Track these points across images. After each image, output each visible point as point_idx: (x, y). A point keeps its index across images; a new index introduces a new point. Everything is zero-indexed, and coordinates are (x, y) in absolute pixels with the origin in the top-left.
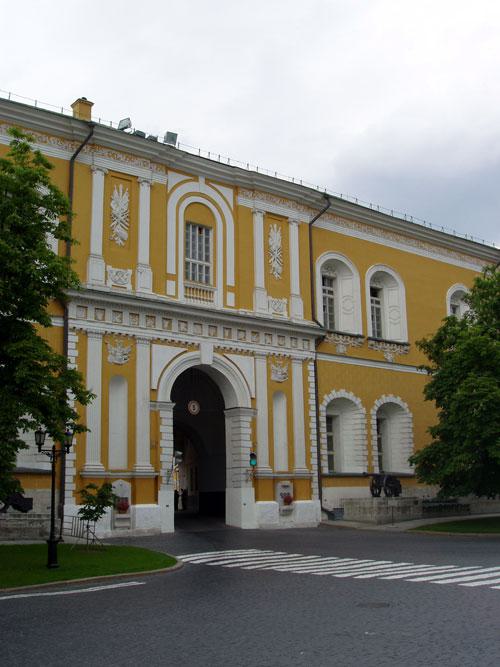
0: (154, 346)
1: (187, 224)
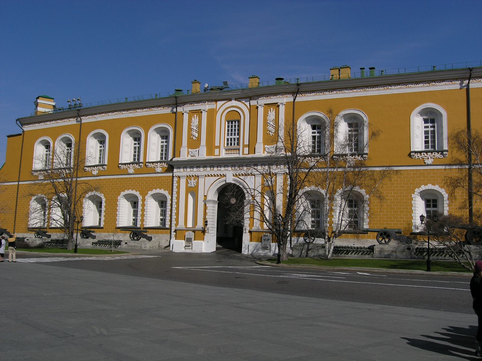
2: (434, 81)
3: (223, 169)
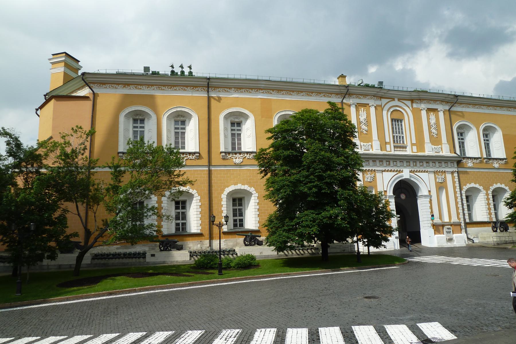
0: (383, 172)
1: (392, 120)
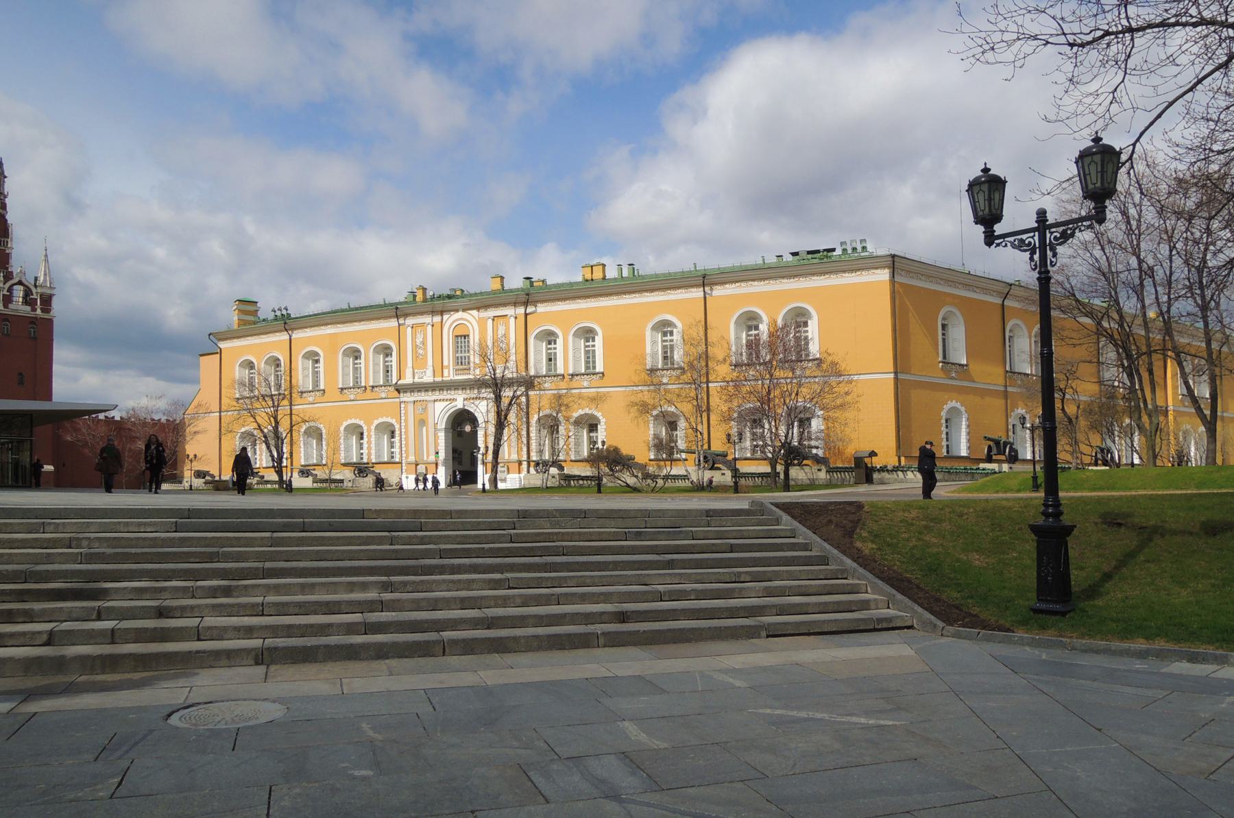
0: (436, 403)
2: (669, 289)
3: (453, 392)
